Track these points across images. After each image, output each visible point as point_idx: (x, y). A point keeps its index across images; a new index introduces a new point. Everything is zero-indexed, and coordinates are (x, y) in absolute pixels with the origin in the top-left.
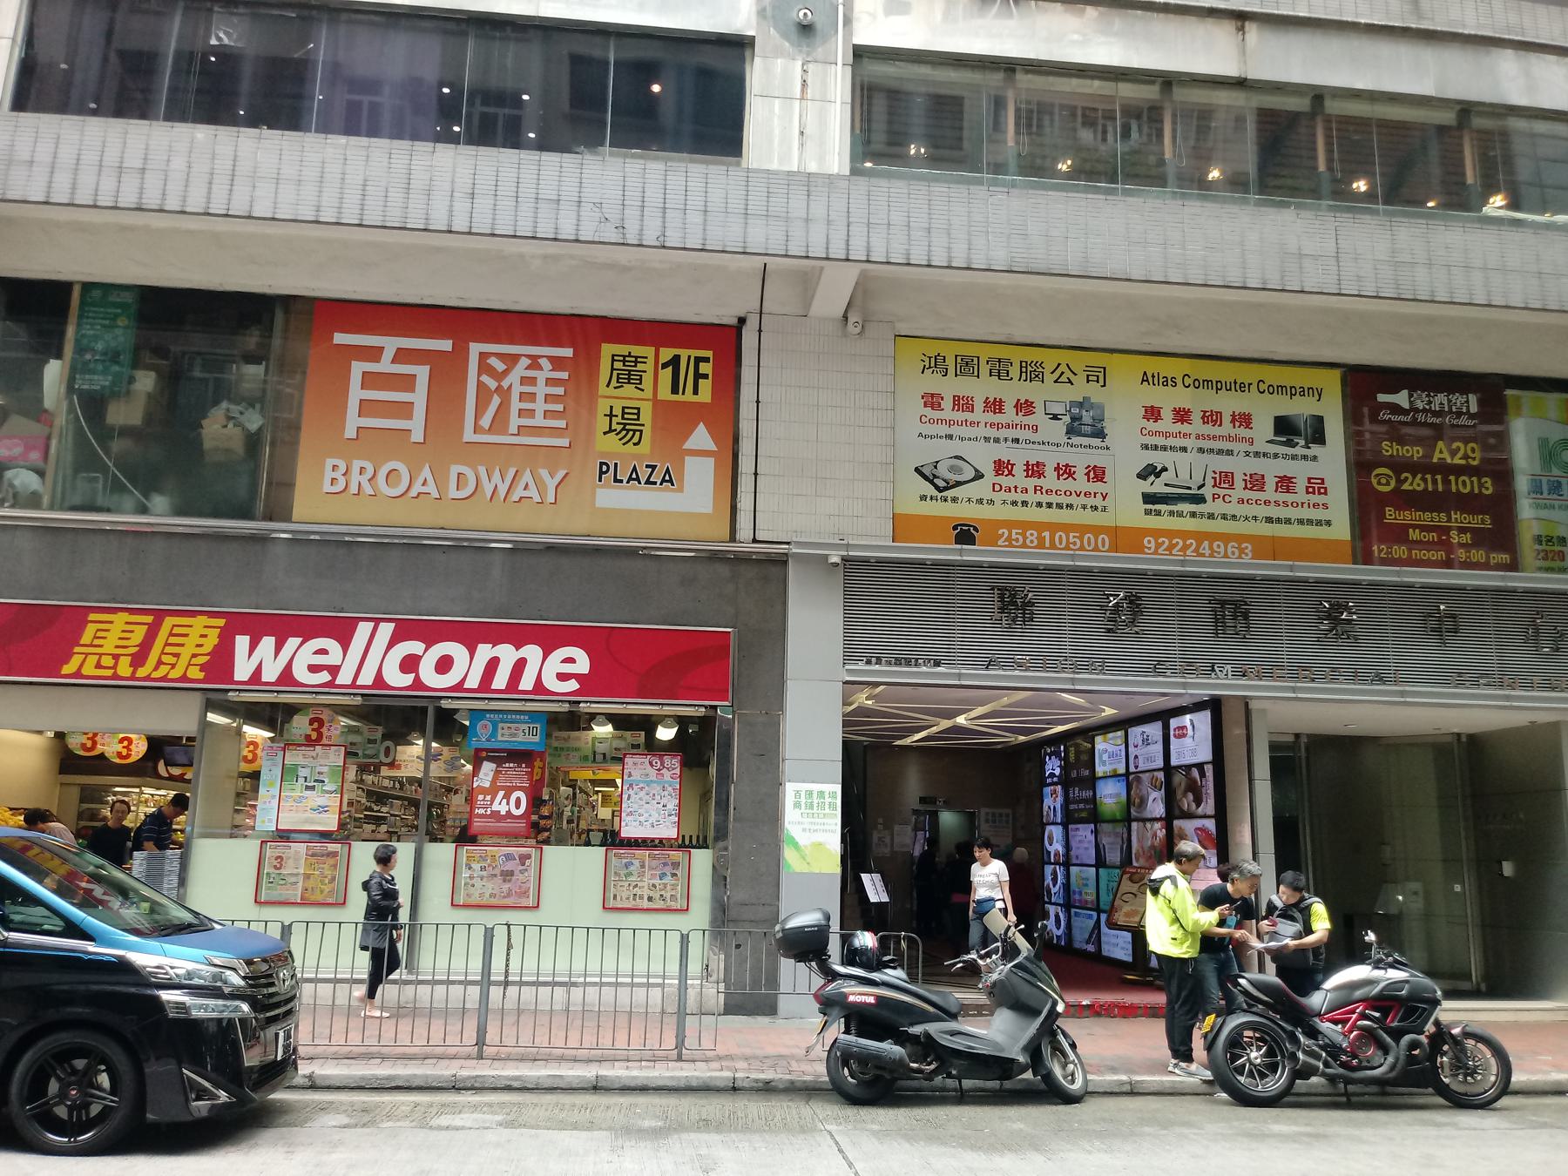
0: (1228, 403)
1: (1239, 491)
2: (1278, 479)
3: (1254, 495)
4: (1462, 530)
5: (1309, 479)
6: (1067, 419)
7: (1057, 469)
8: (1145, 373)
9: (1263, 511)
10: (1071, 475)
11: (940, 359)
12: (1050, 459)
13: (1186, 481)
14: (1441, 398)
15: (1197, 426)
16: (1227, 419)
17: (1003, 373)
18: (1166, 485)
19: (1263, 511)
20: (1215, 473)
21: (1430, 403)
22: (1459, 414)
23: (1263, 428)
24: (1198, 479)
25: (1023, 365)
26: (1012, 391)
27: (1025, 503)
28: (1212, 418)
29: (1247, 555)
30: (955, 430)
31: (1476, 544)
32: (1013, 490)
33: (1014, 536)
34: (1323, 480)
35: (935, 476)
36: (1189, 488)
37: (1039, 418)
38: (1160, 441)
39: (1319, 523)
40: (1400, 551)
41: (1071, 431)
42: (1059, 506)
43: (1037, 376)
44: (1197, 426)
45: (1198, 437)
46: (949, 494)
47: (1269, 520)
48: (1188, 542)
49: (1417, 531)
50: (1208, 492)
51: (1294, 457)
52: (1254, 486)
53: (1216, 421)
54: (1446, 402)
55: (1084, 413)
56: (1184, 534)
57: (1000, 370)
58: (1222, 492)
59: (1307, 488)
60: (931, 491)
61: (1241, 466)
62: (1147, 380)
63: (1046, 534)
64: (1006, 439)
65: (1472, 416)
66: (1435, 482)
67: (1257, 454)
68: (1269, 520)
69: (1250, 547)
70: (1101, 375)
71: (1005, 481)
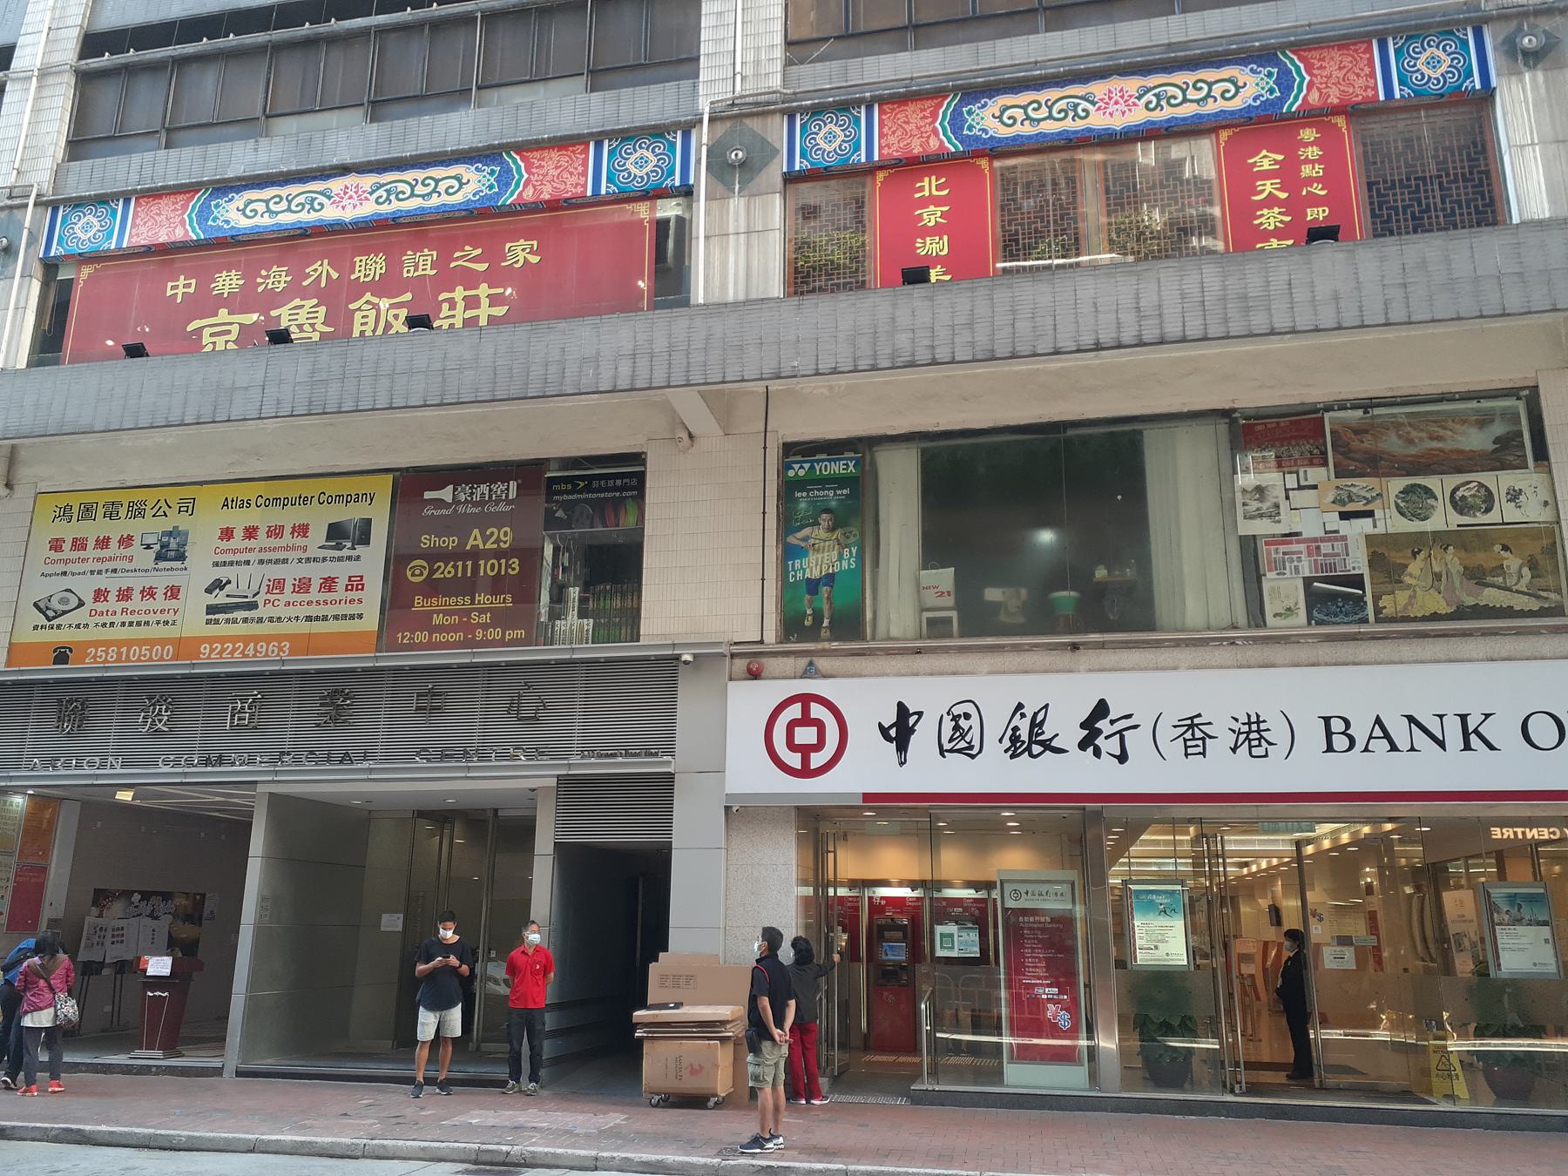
0: (289, 517)
4: (482, 611)
5: (350, 577)
7: (142, 592)
10: (152, 595)
12: (138, 584)
13: (245, 591)
14: (484, 488)
17: (114, 514)
18: (228, 596)
19: (305, 611)
20: (270, 580)
21: (472, 493)
22: (497, 502)
23: (318, 535)
25: (131, 504)
26: (115, 529)
29: (284, 652)
30: (70, 568)
31: (493, 624)
34: (362, 577)
35: (48, 608)
36: (246, 597)
38: (229, 557)
39: (352, 617)
40: (421, 637)
41: (160, 557)
44: (262, 540)
46: (54, 622)
47: (309, 618)
49: (441, 615)
50: (260, 599)
51: (340, 559)
54: (487, 492)
55: (172, 540)
56: (234, 639)
57: (111, 514)
59: (347, 585)
60: (42, 620)
61: (291, 573)
63: (124, 650)
64: (107, 571)
65: (509, 502)
66: (465, 568)
67: (308, 560)
68: (309, 618)
69: (288, 645)
71: (101, 606)
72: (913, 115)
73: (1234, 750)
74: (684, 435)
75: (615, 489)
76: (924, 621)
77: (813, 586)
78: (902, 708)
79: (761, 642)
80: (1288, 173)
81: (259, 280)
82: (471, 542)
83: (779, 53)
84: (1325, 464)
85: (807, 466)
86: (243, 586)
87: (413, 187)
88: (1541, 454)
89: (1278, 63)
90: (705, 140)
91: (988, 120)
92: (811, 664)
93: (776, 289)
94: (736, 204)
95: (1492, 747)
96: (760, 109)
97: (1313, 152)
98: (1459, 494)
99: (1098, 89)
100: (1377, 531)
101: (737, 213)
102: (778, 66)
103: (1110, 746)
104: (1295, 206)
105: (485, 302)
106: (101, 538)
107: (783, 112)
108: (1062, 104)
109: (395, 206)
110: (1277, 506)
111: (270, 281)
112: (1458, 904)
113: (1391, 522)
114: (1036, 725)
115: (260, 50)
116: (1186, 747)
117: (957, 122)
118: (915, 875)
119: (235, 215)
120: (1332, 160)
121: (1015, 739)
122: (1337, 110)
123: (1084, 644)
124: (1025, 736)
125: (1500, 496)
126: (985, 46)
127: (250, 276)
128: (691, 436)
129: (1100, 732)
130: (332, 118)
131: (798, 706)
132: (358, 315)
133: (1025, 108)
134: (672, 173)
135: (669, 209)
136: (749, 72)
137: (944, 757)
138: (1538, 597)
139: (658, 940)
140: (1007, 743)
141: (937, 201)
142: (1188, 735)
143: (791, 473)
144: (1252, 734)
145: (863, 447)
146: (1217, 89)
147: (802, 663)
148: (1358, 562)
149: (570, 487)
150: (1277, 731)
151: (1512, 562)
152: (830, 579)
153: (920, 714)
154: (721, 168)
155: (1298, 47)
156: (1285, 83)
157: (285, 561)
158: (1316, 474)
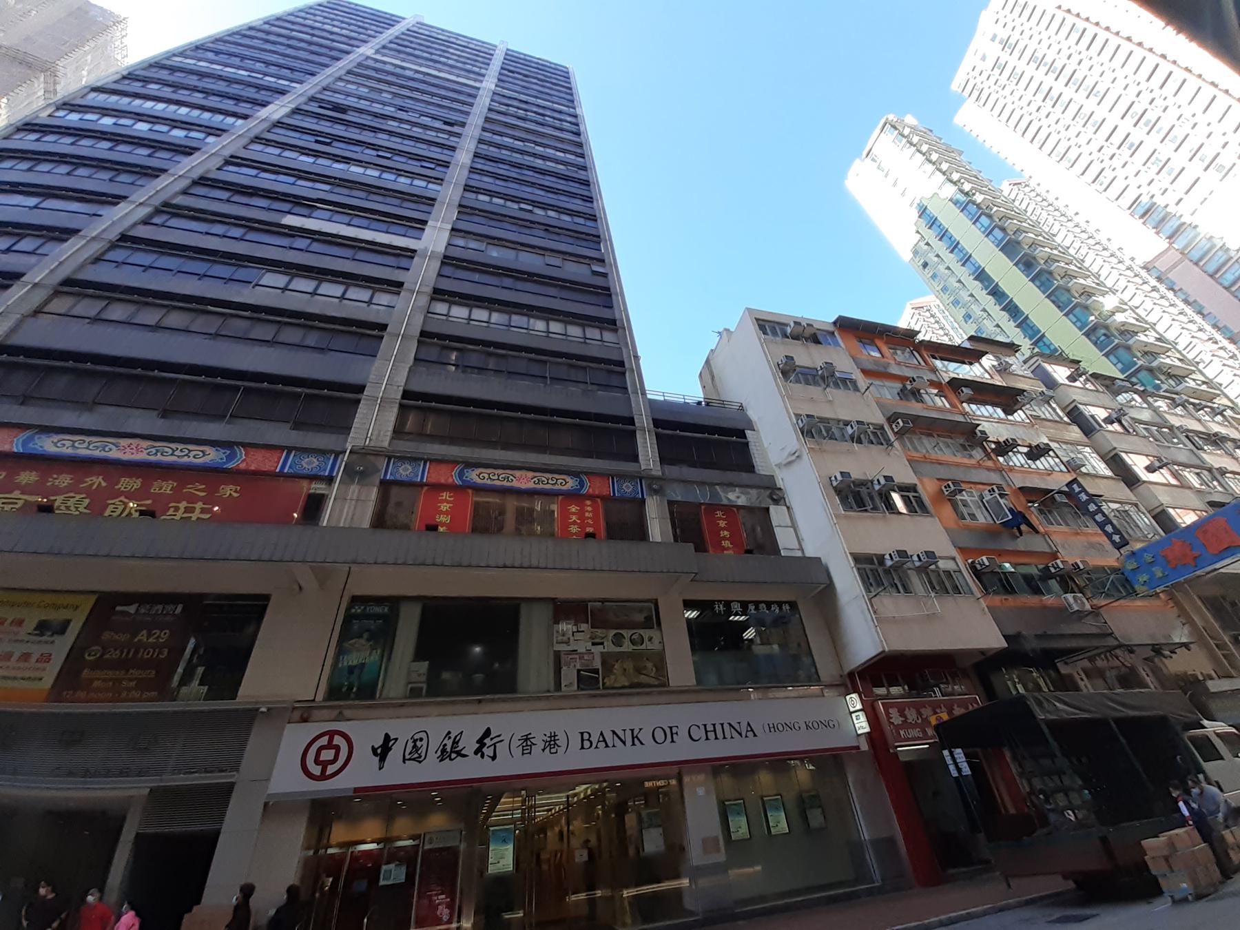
4: (131, 680)
14: (160, 607)
72: (443, 469)
73: (543, 750)
74: (297, 588)
76: (420, 685)
77: (351, 670)
78: (387, 736)
79: (314, 700)
80: (581, 515)
81: (51, 480)
82: (139, 637)
83: (389, 434)
84: (588, 623)
85: (362, 607)
87: (174, 451)
88: (659, 624)
89: (580, 478)
90: (345, 459)
91: (474, 476)
92: (341, 713)
93: (366, 524)
94: (354, 490)
95: (642, 744)
96: (377, 453)
97: (589, 509)
98: (633, 637)
99: (518, 473)
100: (605, 650)
101: (354, 491)
102: (388, 439)
103: (488, 751)
104: (582, 526)
105: (198, 510)
107: (386, 456)
108: (503, 476)
109: (159, 457)
110: (569, 639)
111: (57, 481)
112: (630, 820)
113: (609, 647)
114: (455, 742)
115: (104, 374)
116: (523, 750)
117: (461, 475)
118: (378, 836)
119: (49, 445)
120: (595, 511)
121: (444, 751)
122: (598, 497)
123: (484, 699)
124: (449, 750)
125: (646, 639)
126: (477, 450)
128: (300, 588)
129: (485, 744)
130: (137, 412)
131: (327, 738)
132: (111, 508)
133: (489, 474)
134: (325, 470)
135: (318, 488)
136: (374, 438)
137: (404, 762)
138: (659, 679)
139: (198, 902)
140: (439, 753)
141: (448, 502)
142: (524, 744)
143: (353, 611)
144: (552, 742)
145: (394, 602)
146: (559, 482)
147: (336, 712)
148: (597, 664)
150: (562, 741)
151: (650, 665)
152: (363, 665)
153: (396, 739)
154: (350, 473)
155: (586, 474)
156: (582, 484)
158: (584, 627)
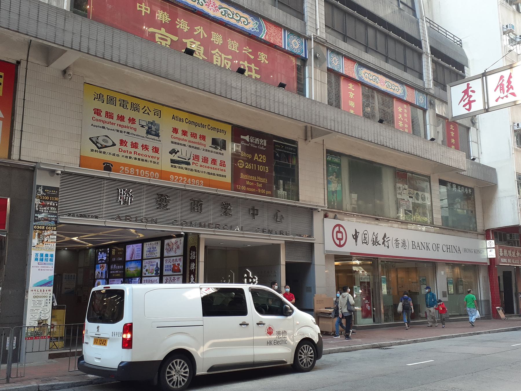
0: (199, 131)
1: (200, 163)
2: (212, 160)
3: (205, 164)
4: (260, 183)
5: (221, 161)
6: (147, 128)
7: (142, 146)
8: (174, 115)
9: (207, 170)
10: (147, 149)
11: (101, 96)
13: (184, 157)
14: (257, 140)
15: (189, 137)
16: (198, 136)
18: (178, 157)
19: (207, 170)
21: (254, 141)
23: (208, 142)
24: (188, 156)
26: (128, 113)
27: (130, 157)
28: (194, 135)
30: (106, 125)
32: (126, 152)
33: (126, 170)
35: (97, 142)
36: (186, 159)
37: (137, 126)
38: (177, 141)
39: (223, 176)
41: (148, 133)
42: (143, 160)
43: (137, 109)
44: (189, 137)
45: (189, 142)
47: (209, 173)
48: (184, 178)
50: (191, 161)
51: (217, 153)
52: (205, 161)
53: (195, 137)
54: (258, 141)
55: (153, 127)
56: (183, 175)
57: (123, 104)
58: (195, 162)
62: (174, 118)
63: (137, 170)
65: (264, 147)
66: (254, 166)
68: (209, 173)
70: (159, 113)
75: (290, 151)
77: (333, 192)
86: (184, 154)
92: (336, 215)
106: (131, 118)
127: (225, 39)
149: (279, 146)
157: (198, 148)
